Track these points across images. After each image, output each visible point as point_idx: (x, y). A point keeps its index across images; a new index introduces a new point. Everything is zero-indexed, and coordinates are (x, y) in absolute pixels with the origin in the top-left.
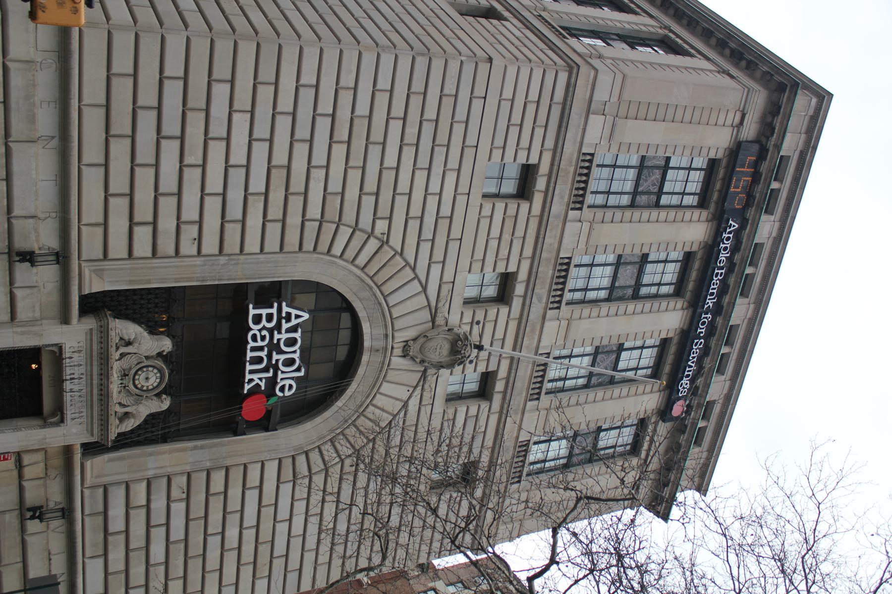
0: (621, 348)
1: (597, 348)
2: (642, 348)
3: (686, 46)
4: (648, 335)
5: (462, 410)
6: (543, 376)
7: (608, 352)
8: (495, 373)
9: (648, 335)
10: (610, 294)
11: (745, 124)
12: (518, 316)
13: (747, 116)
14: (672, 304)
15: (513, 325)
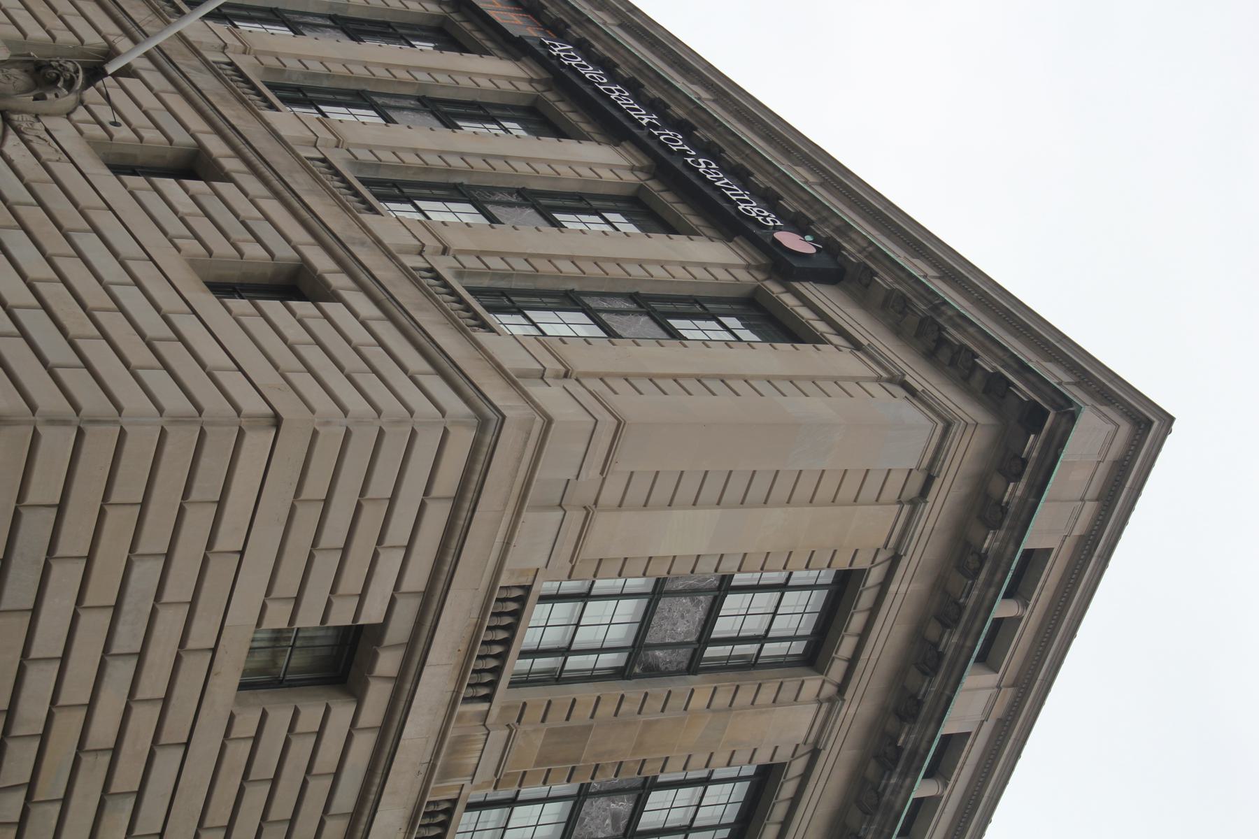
0: (725, 586)
1: (660, 582)
2: (783, 588)
3: (805, 313)
4: (799, 560)
5: (279, 718)
6: (507, 643)
7: (692, 592)
8: (377, 632)
9: (799, 560)
10: (630, 661)
11: (930, 498)
12: (452, 492)
13: (938, 482)
14: (791, 686)
15: (363, 746)
